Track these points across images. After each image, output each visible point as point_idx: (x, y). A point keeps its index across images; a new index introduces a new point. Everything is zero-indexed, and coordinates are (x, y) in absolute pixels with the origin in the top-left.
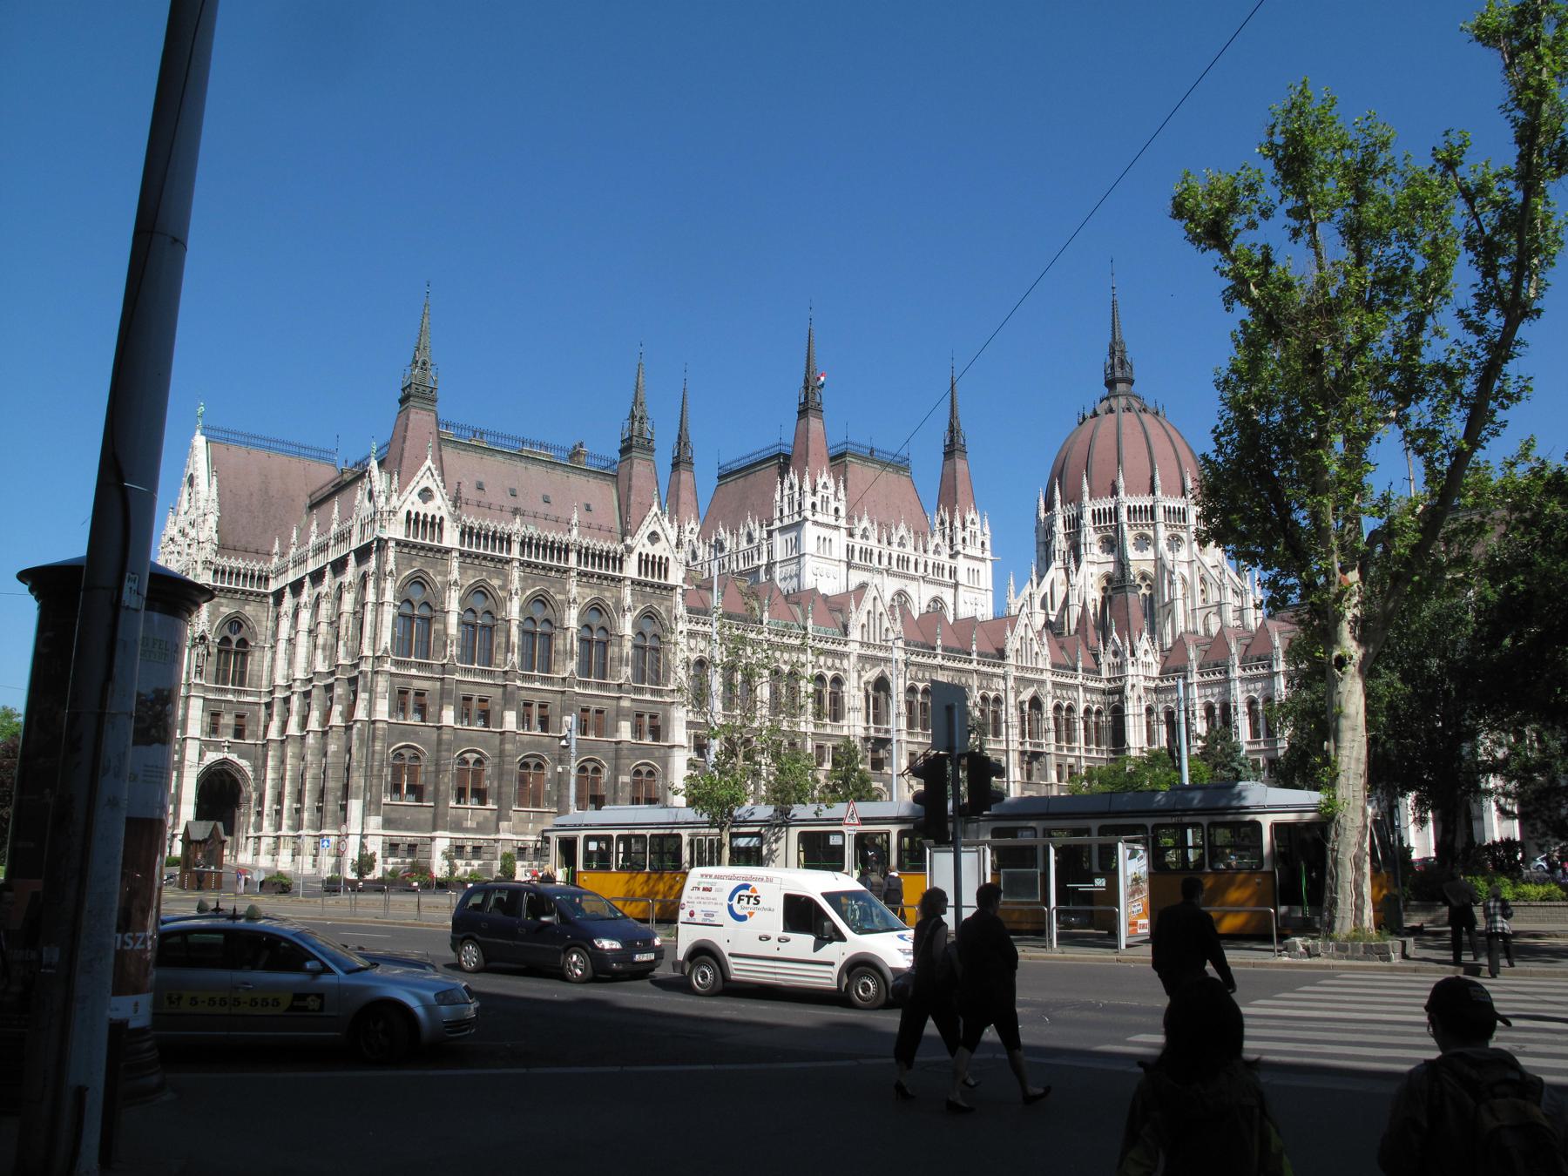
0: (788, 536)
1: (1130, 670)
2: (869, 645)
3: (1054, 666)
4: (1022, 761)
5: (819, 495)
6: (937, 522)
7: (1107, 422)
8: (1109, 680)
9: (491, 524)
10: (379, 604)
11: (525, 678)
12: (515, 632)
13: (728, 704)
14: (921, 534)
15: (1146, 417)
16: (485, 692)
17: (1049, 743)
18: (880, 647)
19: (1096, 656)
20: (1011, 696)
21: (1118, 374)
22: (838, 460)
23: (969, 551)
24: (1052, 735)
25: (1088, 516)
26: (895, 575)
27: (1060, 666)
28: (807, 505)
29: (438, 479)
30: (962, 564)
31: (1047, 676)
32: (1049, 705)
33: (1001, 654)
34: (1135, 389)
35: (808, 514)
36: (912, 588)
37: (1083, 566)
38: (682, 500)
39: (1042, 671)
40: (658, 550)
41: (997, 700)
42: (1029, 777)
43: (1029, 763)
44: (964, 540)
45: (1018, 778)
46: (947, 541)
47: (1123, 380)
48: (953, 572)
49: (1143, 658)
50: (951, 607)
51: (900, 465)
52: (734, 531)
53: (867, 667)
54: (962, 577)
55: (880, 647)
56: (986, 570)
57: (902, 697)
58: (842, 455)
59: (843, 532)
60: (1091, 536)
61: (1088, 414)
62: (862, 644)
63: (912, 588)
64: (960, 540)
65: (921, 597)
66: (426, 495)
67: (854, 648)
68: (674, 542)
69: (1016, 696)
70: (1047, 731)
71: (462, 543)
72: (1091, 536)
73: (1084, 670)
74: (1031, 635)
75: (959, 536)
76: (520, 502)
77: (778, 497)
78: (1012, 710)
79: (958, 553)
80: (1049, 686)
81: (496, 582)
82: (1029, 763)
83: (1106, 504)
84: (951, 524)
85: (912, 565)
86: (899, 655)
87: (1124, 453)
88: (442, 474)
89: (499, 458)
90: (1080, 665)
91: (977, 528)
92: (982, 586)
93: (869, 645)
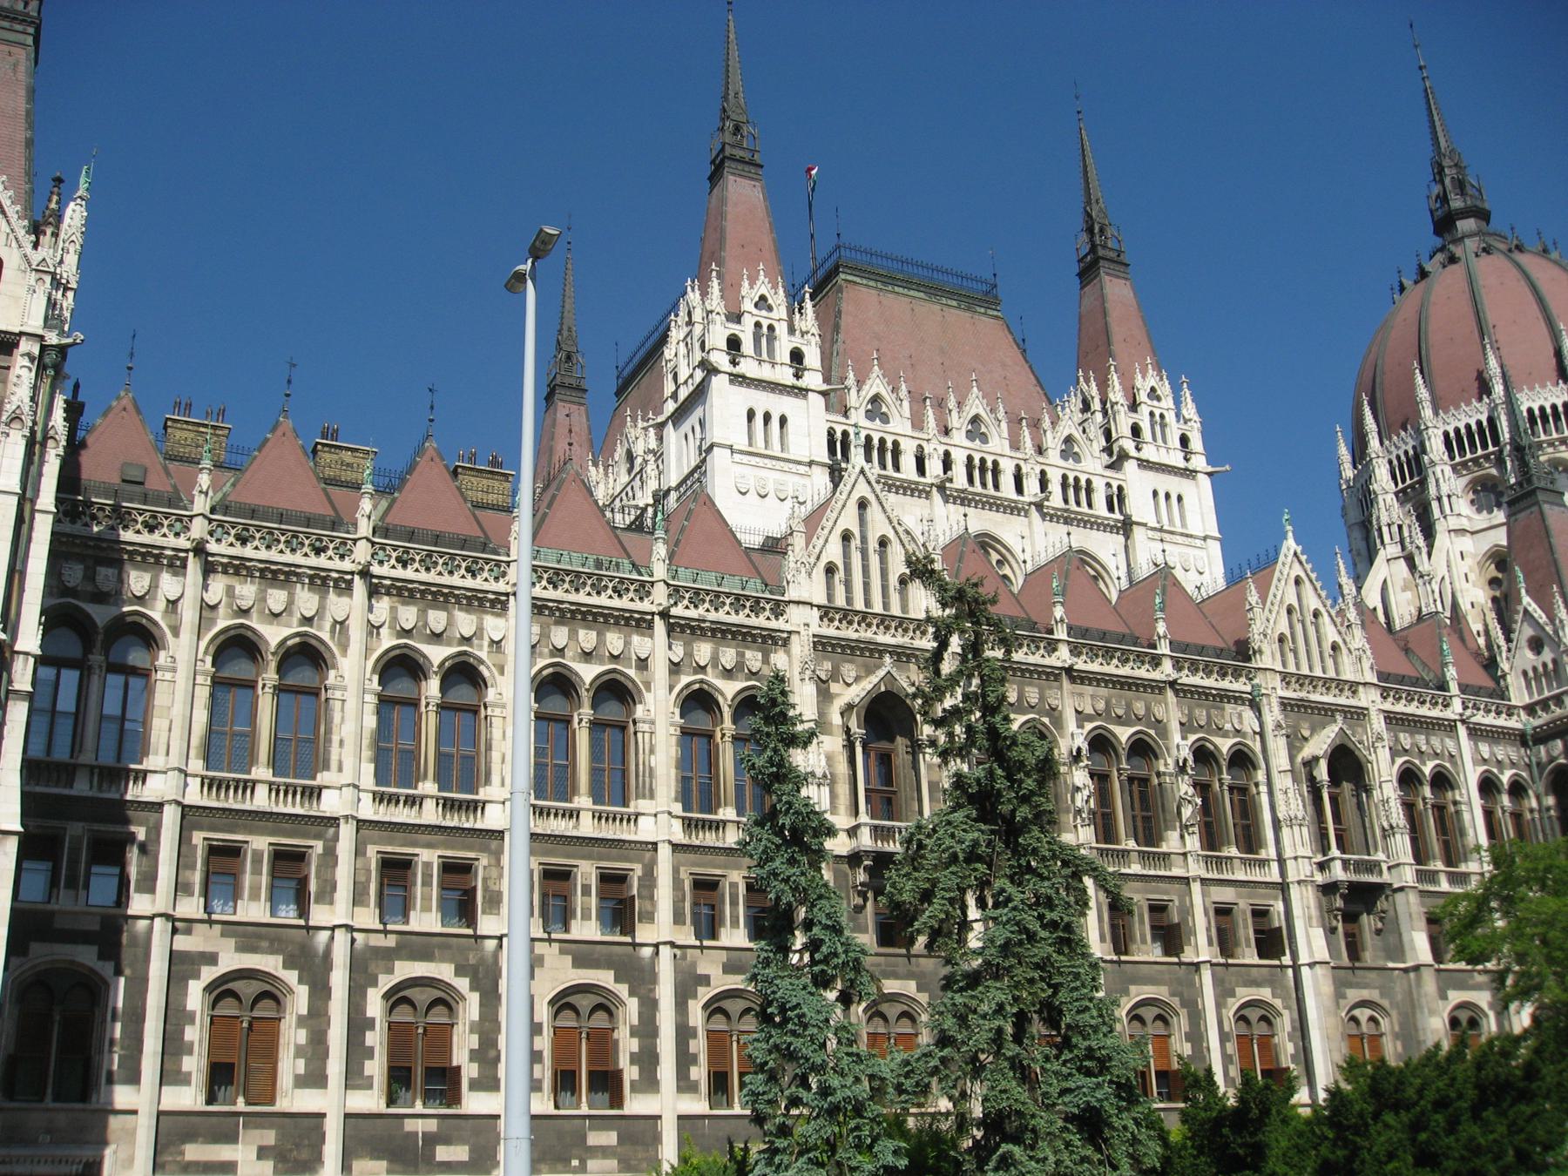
0: (686, 427)
2: (847, 615)
3: (1383, 676)
4: (1327, 912)
7: (1447, 283)
8: (1530, 709)
13: (393, 762)
15: (1517, 256)
17: (1396, 860)
18: (884, 621)
19: (1491, 664)
21: (1456, 203)
22: (818, 283)
23: (1149, 453)
24: (1402, 844)
25: (1436, 447)
26: (963, 499)
27: (1401, 680)
31: (1369, 699)
32: (1383, 769)
33: (1244, 651)
34: (1496, 223)
35: (721, 359)
36: (1008, 529)
37: (1442, 539)
39: (1354, 687)
42: (1354, 950)
43: (1350, 918)
44: (1136, 431)
45: (1322, 953)
46: (1095, 431)
47: (1465, 213)
48: (1117, 499)
51: (980, 296)
53: (849, 671)
54: (1139, 506)
55: (884, 621)
56: (1200, 502)
58: (834, 272)
59: (816, 401)
60: (1447, 481)
61: (1407, 283)
62: (827, 612)
63: (1008, 529)
64: (1128, 433)
67: (802, 623)
69: (1292, 751)
70: (1388, 832)
72: (1447, 483)
73: (1464, 688)
74: (1312, 602)
78: (1283, 782)
80: (1378, 723)
82: (1350, 918)
83: (1472, 414)
84: (1104, 402)
85: (1007, 481)
87: (1490, 317)
90: (1451, 673)
91: (1167, 415)
92: (1195, 527)
93: (847, 615)
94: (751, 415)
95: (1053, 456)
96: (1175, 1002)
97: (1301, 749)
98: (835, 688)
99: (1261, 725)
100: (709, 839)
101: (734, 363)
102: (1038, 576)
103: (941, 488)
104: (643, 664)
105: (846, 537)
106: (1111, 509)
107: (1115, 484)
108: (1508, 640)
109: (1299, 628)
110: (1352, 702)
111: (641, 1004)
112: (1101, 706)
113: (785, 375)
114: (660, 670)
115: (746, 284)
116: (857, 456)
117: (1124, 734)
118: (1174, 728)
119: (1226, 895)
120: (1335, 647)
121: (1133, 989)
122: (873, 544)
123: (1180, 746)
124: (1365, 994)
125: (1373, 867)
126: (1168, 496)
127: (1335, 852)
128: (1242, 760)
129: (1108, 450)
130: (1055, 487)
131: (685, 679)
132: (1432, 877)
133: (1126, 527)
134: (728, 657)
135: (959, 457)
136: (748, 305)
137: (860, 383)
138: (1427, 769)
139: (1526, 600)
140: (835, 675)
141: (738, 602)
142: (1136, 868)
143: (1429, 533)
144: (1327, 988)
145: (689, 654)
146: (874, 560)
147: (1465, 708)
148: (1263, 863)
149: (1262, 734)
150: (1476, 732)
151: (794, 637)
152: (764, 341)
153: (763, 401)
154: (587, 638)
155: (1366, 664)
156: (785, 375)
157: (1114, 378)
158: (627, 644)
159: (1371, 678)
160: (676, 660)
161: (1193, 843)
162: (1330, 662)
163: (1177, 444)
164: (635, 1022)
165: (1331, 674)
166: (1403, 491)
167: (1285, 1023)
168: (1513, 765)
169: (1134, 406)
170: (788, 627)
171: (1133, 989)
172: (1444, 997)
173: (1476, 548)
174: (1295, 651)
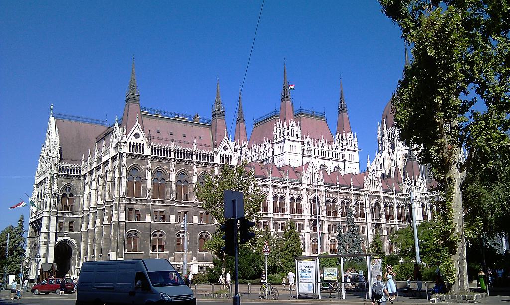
1: (415, 191)
5: (290, 129)
6: (337, 137)
8: (406, 195)
9: (162, 146)
10: (120, 178)
11: (178, 203)
12: (173, 185)
14: (330, 143)
16: (163, 209)
20: (367, 202)
22: (297, 116)
26: (320, 158)
28: (286, 133)
29: (141, 130)
30: (346, 153)
31: (381, 194)
32: (382, 205)
36: (327, 163)
38: (241, 134)
40: (227, 153)
41: (362, 204)
46: (341, 145)
48: (343, 156)
49: (420, 186)
50: (343, 169)
51: (322, 117)
52: (260, 145)
53: (310, 193)
54: (346, 158)
56: (356, 155)
57: (324, 204)
63: (327, 163)
64: (345, 144)
65: (331, 166)
66: (137, 136)
68: (233, 149)
71: (152, 154)
74: (374, 178)
76: (174, 137)
77: (275, 131)
79: (345, 149)
80: (382, 198)
81: (165, 167)
82: (376, 228)
84: (342, 138)
86: (322, 188)
88: (143, 127)
89: (166, 121)
90: (394, 189)
91: (352, 139)
95: (334, 150)
98: (309, 196)
100: (294, 218)
103: (318, 157)
114: (288, 194)
118: (353, 200)
120: (377, 185)
122: (314, 174)
125: (380, 221)
127: (374, 218)
134: (296, 192)
135: (320, 151)
139: (408, 177)
143: (393, 149)
146: (314, 176)
150: (397, 199)
157: (344, 134)
165: (376, 190)
173: (402, 153)
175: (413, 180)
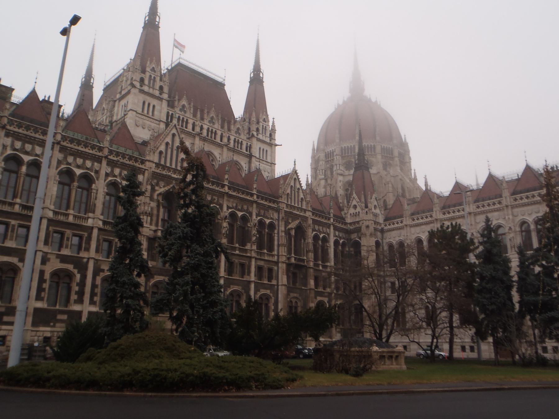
2: (164, 167)
3: (313, 209)
5: (148, 74)
23: (260, 136)
24: (311, 255)
31: (308, 214)
32: (310, 234)
39: (305, 211)
42: (294, 283)
44: (258, 130)
48: (249, 148)
53: (162, 184)
54: (255, 152)
59: (165, 104)
62: (158, 165)
63: (216, 152)
67: (150, 167)
69: (286, 226)
73: (334, 216)
75: (254, 127)
79: (253, 135)
80: (310, 222)
84: (250, 120)
94: (144, 103)
96: (243, 291)
97: (288, 226)
98: (157, 188)
99: (279, 217)
101: (141, 86)
102: (223, 165)
104: (97, 172)
105: (167, 144)
106: (247, 151)
107: (249, 144)
108: (348, 205)
109: (293, 192)
110: (304, 215)
111: (81, 276)
112: (235, 205)
113: (157, 93)
115: (149, 62)
116: (175, 121)
117: (240, 214)
119: (261, 263)
121: (232, 286)
123: (255, 219)
124: (295, 295)
125: (303, 260)
126: (263, 150)
127: (293, 255)
128: (272, 226)
129: (249, 133)
130: (232, 142)
131: (110, 179)
132: (317, 265)
133: (250, 156)
136: (148, 69)
137: (179, 100)
138: (321, 236)
140: (157, 184)
141: (131, 158)
142: (237, 252)
144: (285, 292)
145: (112, 171)
147: (334, 221)
148: (273, 256)
149: (278, 220)
151: (146, 171)
152: (152, 81)
153: (149, 99)
154: (80, 161)
155: (309, 205)
156: (157, 93)
157: (254, 114)
158: (93, 165)
159: (310, 209)
160: (108, 172)
161: (254, 247)
162: (300, 203)
163: (268, 136)
164: (78, 281)
165: (300, 206)
166: (328, 161)
167: (273, 300)
168: (344, 238)
169: (258, 123)
170: (145, 168)
171: (232, 286)
172: (316, 298)
174: (291, 199)
175: (363, 200)
